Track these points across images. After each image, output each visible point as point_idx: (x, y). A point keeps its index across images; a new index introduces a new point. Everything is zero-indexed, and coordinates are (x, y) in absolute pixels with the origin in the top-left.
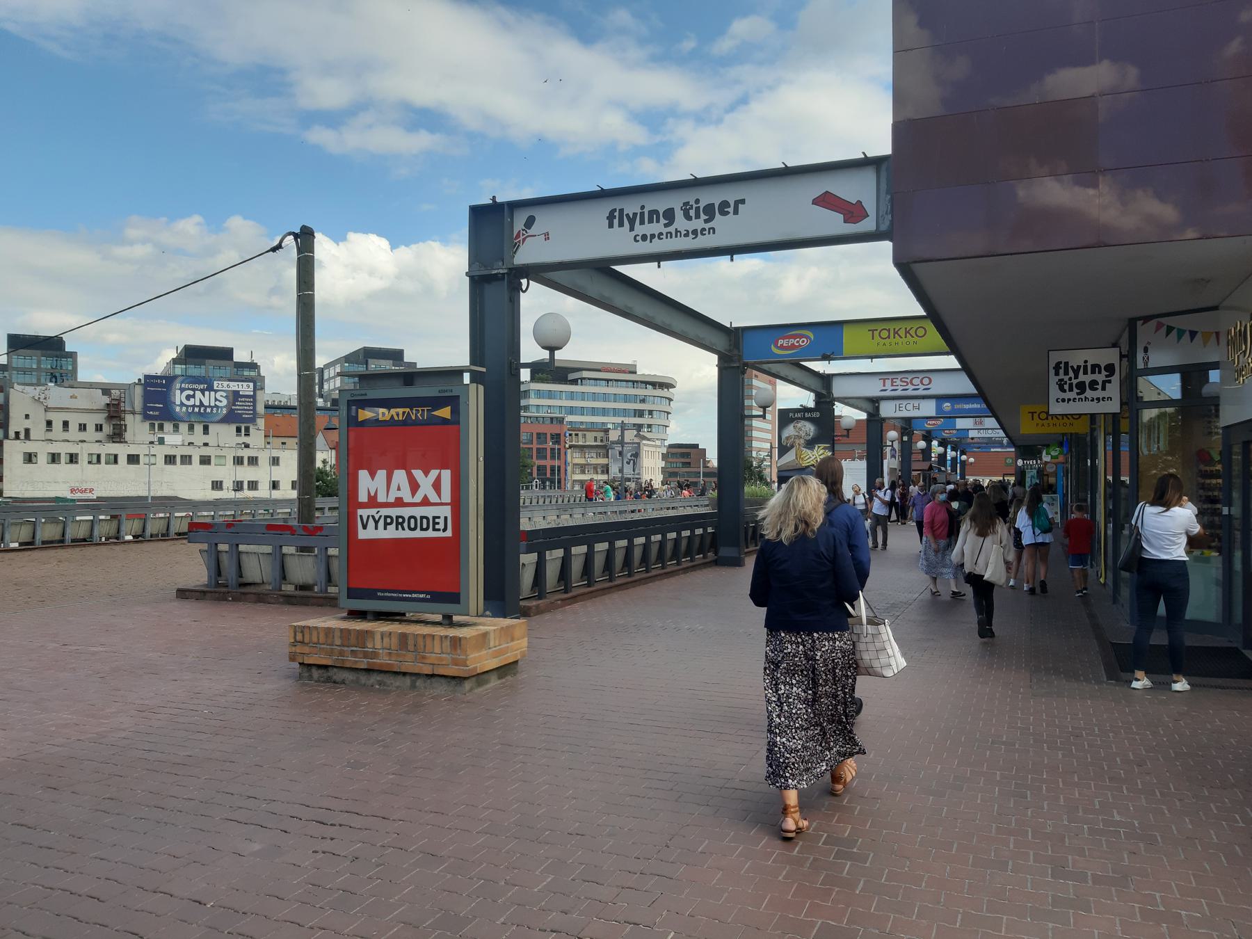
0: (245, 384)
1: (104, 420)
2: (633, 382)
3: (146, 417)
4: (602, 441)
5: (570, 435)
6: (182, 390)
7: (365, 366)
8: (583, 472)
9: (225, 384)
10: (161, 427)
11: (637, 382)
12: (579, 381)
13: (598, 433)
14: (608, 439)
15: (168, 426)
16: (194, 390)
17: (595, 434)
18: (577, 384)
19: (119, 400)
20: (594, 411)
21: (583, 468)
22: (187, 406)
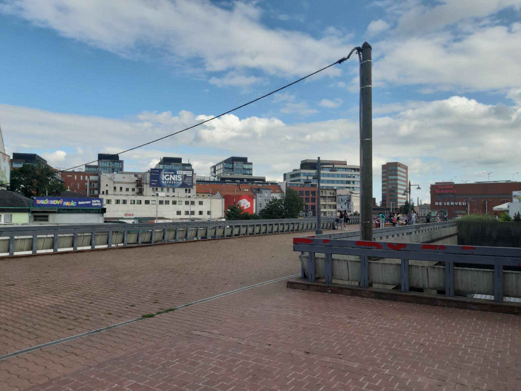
0: (189, 172)
1: (135, 187)
2: (346, 168)
3: (151, 185)
4: (333, 194)
6: (165, 174)
7: (232, 164)
8: (325, 208)
9: (181, 172)
10: (157, 189)
11: (347, 168)
13: (331, 191)
14: (336, 194)
15: (159, 189)
16: (169, 174)
17: (330, 191)
19: (141, 179)
22: (167, 181)
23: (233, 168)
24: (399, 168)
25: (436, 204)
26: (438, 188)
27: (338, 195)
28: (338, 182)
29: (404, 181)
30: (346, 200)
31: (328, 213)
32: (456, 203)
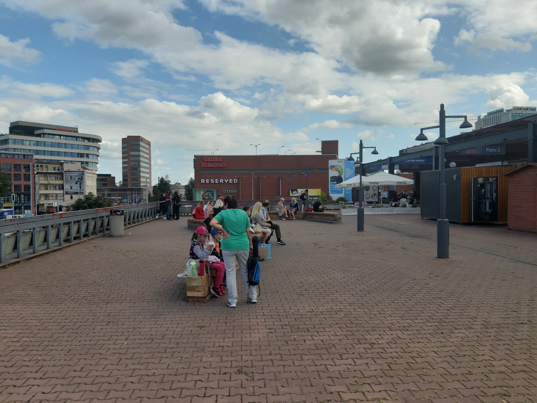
2: (77, 137)
5: (37, 166)
8: (46, 189)
11: (79, 137)
12: (42, 135)
13: (56, 165)
14: (63, 169)
20: (52, 153)
21: (46, 187)
24: (141, 143)
25: (202, 181)
26: (205, 160)
27: (65, 171)
28: (66, 154)
29: (146, 158)
30: (77, 178)
31: (52, 196)
32: (226, 180)
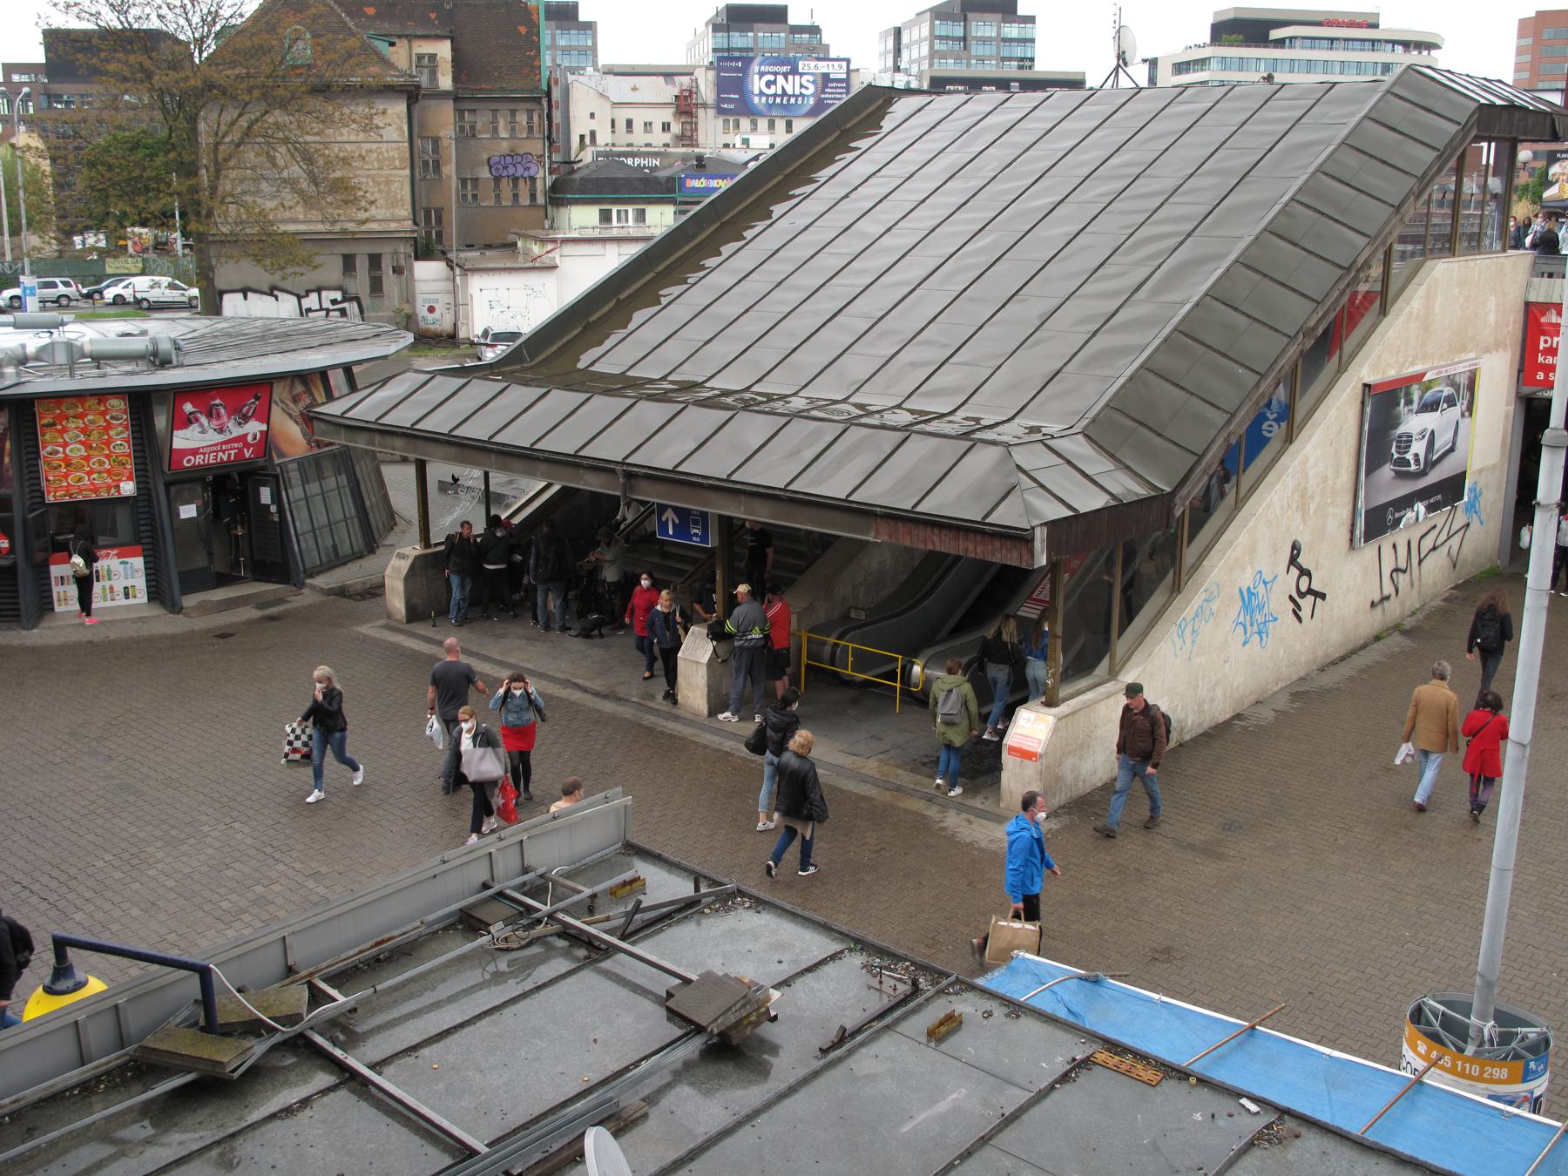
0: (836, 64)
2: (1373, 41)
3: (721, 111)
6: (761, 74)
9: (813, 64)
10: (737, 126)
12: (1287, 41)
15: (745, 123)
16: (775, 74)
18: (1283, 47)
19: (691, 91)
22: (768, 96)
23: (964, 39)
